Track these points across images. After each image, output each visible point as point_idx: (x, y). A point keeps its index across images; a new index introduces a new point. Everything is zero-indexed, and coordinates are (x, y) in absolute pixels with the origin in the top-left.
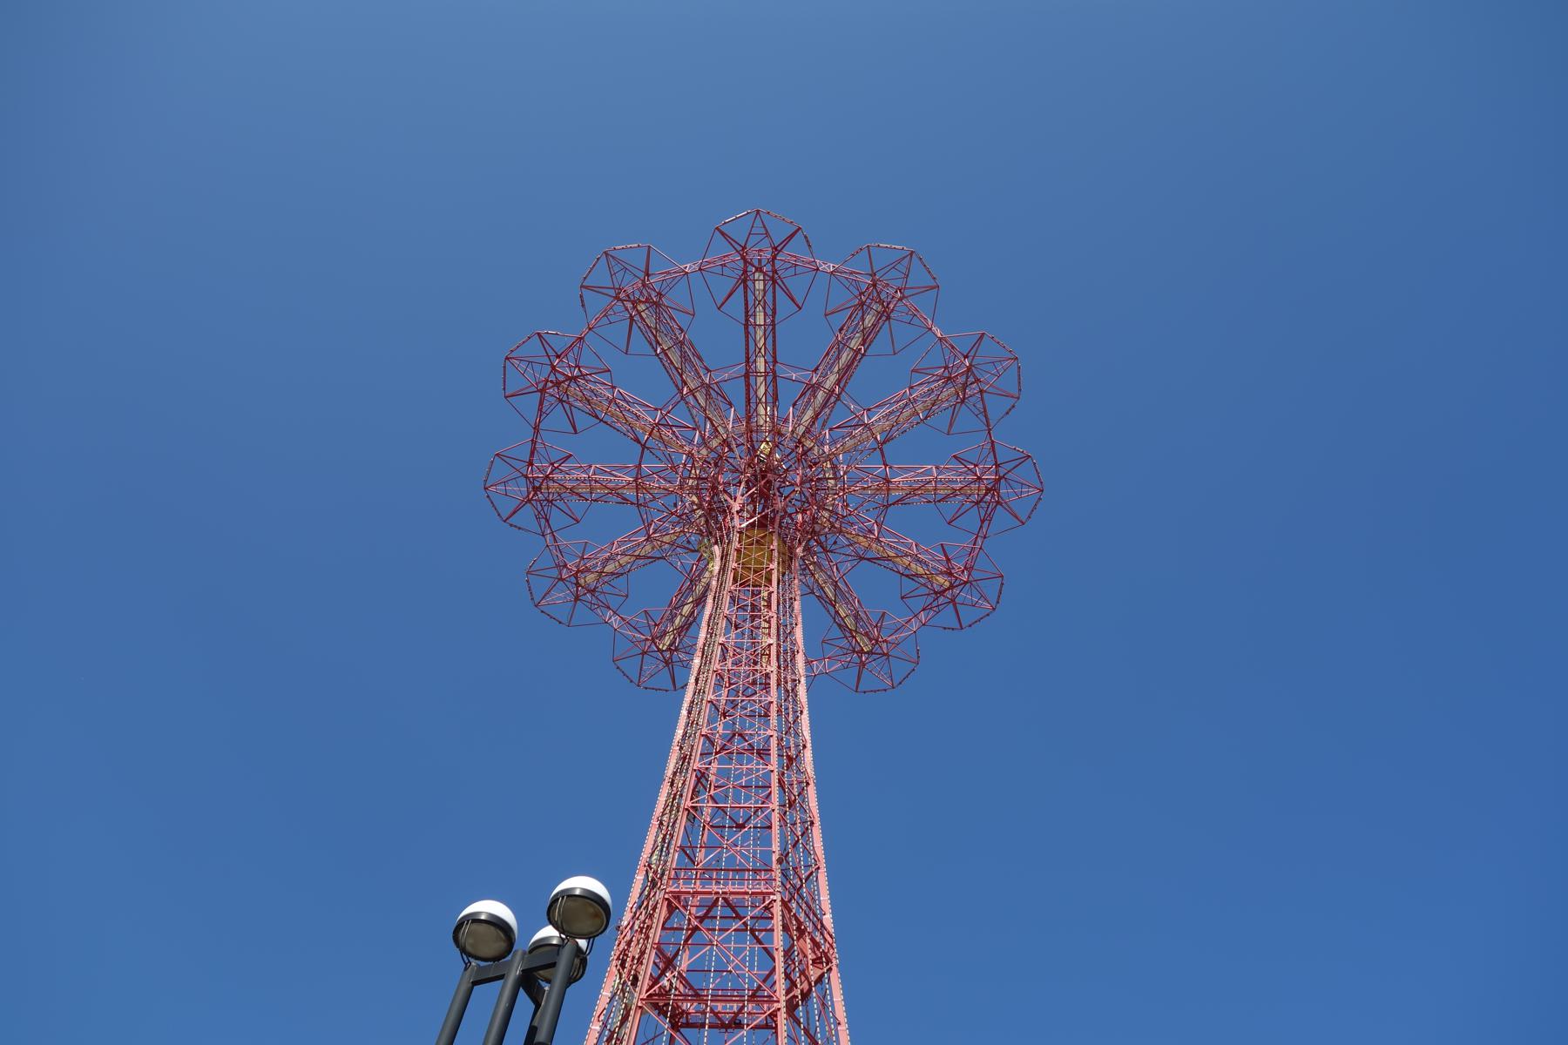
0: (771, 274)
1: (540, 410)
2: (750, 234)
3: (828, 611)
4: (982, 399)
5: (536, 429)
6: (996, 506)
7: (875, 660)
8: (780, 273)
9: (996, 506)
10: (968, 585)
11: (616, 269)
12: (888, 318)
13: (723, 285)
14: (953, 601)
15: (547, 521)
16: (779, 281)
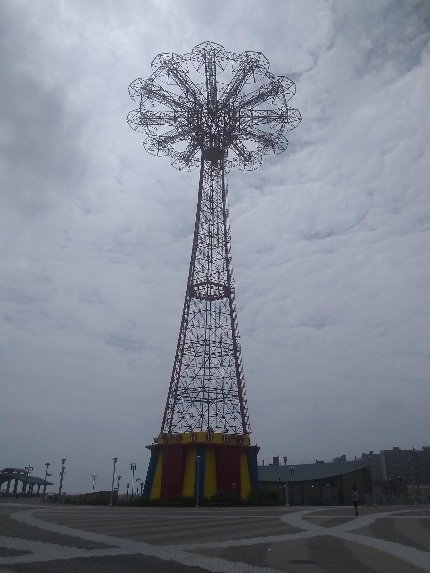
5: (141, 105)
12: (253, 73)
13: (197, 64)
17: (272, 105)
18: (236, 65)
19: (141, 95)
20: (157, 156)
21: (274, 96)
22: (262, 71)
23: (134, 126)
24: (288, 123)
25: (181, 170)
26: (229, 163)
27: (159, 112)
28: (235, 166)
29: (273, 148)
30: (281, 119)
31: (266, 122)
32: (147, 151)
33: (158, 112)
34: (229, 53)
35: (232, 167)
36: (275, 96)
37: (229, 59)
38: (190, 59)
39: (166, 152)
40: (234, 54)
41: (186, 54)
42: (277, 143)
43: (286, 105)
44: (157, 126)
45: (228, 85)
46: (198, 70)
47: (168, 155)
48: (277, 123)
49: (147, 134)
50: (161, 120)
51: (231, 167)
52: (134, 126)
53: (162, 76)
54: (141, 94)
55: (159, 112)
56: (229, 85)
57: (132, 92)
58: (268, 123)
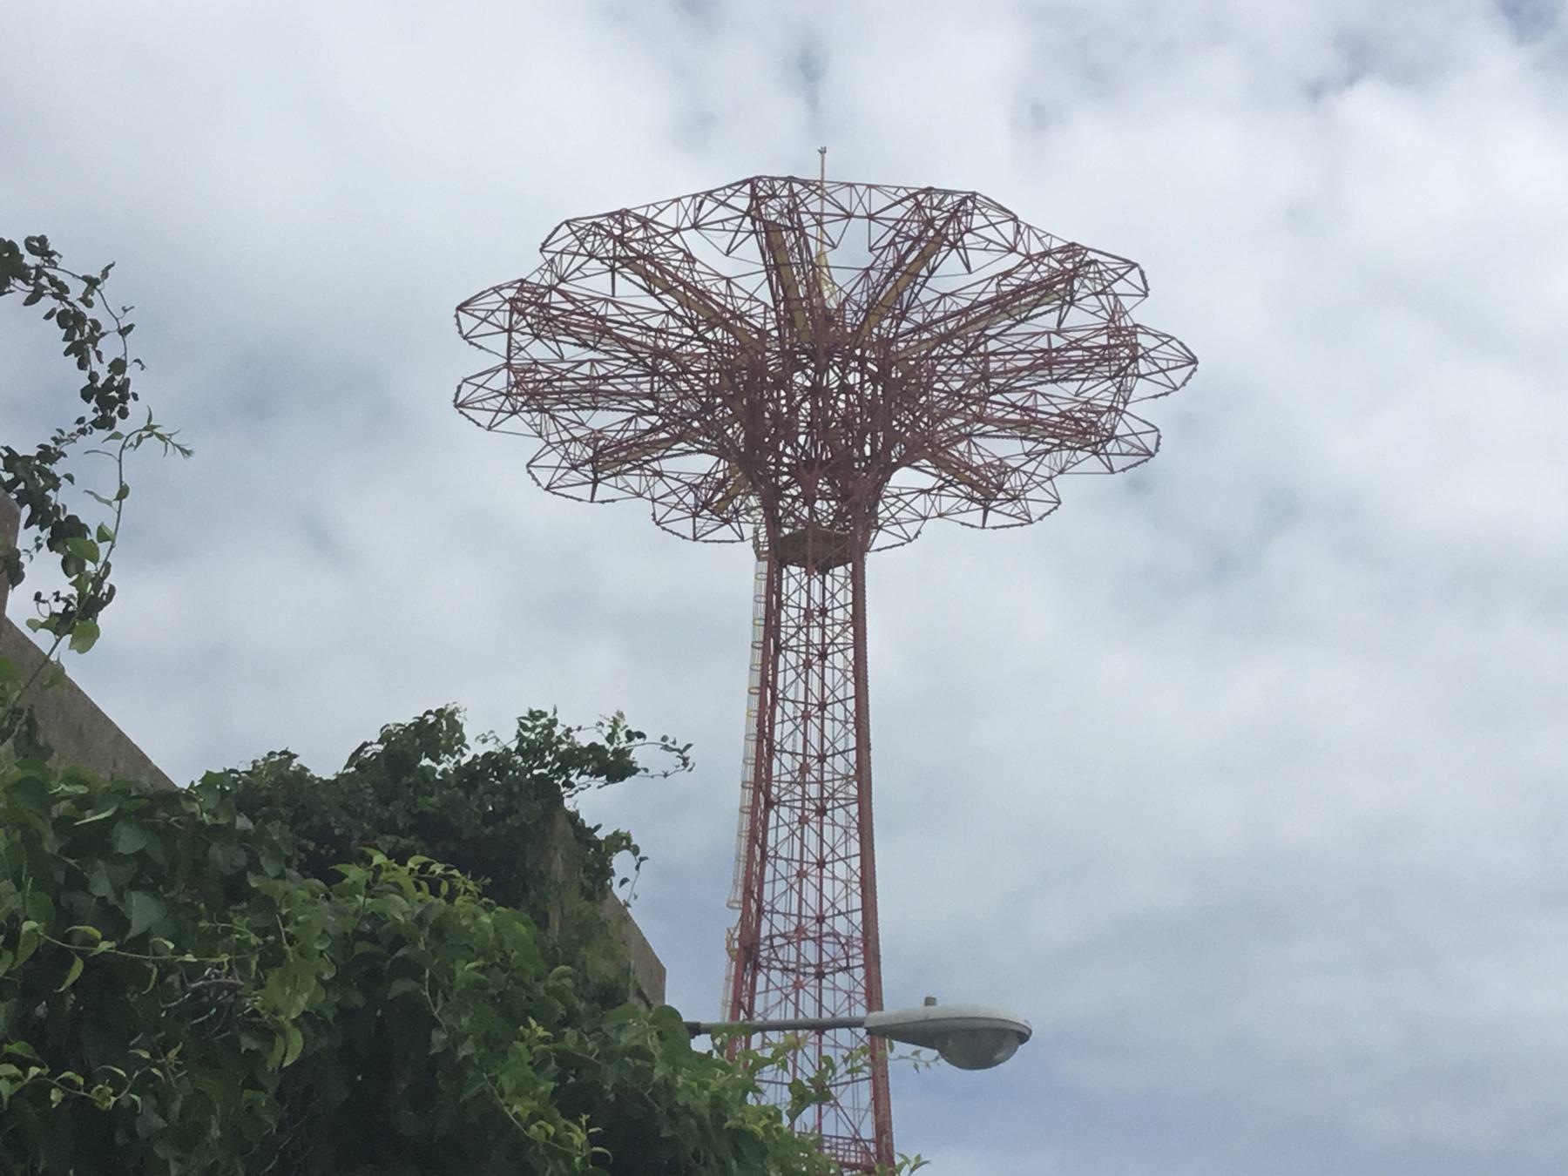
13: (724, 241)
18: (878, 230)
19: (505, 331)
20: (592, 501)
22: (990, 241)
24: (1143, 376)
25: (704, 538)
26: (907, 504)
27: (589, 364)
28: (940, 515)
30: (1109, 366)
31: (1049, 378)
32: (547, 489)
33: (581, 363)
34: (851, 185)
35: (928, 521)
37: (849, 216)
38: (695, 226)
39: (628, 486)
40: (873, 190)
41: (678, 200)
44: (584, 415)
46: (728, 253)
47: (639, 495)
48: (1093, 379)
49: (540, 436)
50: (594, 394)
51: (925, 518)
52: (485, 418)
53: (586, 276)
54: (507, 327)
55: (589, 364)
56: (867, 270)
57: (468, 322)
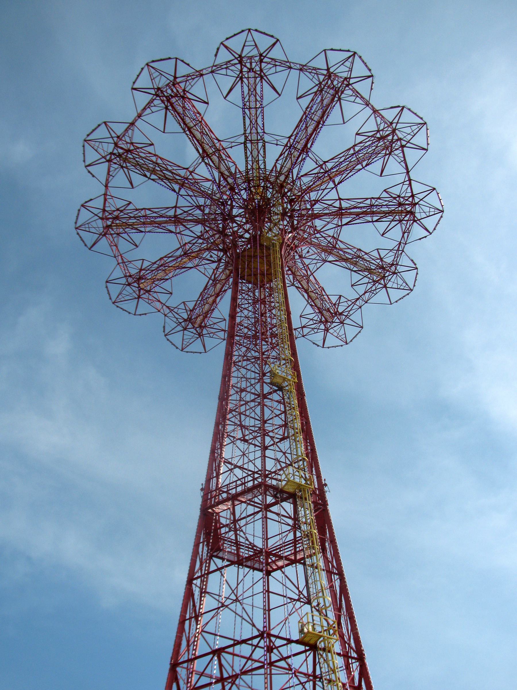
0: (259, 72)
1: (108, 173)
2: (244, 46)
3: (304, 296)
4: (403, 152)
5: (106, 186)
6: (413, 223)
7: (335, 327)
8: (265, 71)
9: (413, 223)
10: (395, 275)
11: (155, 75)
13: (226, 82)
14: (385, 286)
15: (117, 247)
16: (265, 78)
17: (381, 176)
21: (386, 155)
23: (90, 238)
28: (303, 336)
29: (385, 286)
36: (388, 154)
42: (394, 273)
43: (409, 177)
45: (288, 138)
47: (159, 311)
53: (153, 112)
58: (372, 222)
